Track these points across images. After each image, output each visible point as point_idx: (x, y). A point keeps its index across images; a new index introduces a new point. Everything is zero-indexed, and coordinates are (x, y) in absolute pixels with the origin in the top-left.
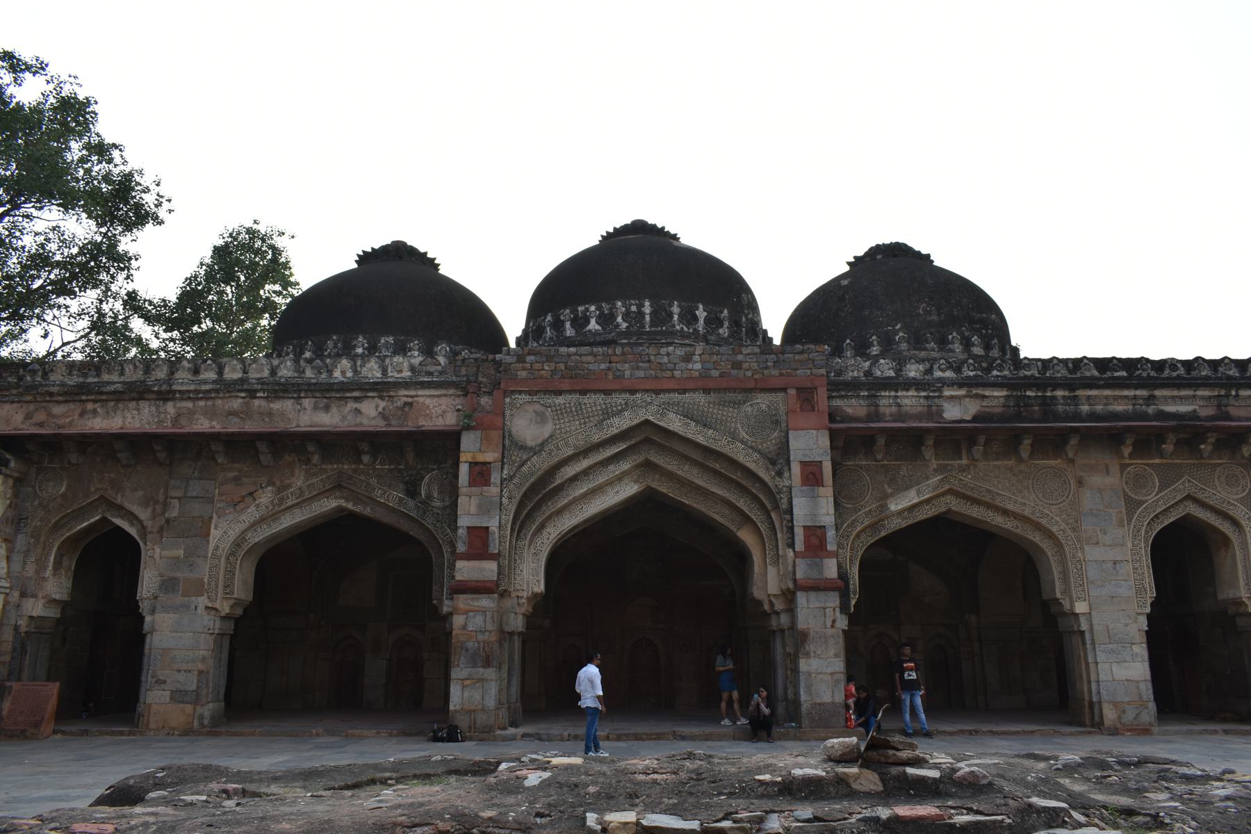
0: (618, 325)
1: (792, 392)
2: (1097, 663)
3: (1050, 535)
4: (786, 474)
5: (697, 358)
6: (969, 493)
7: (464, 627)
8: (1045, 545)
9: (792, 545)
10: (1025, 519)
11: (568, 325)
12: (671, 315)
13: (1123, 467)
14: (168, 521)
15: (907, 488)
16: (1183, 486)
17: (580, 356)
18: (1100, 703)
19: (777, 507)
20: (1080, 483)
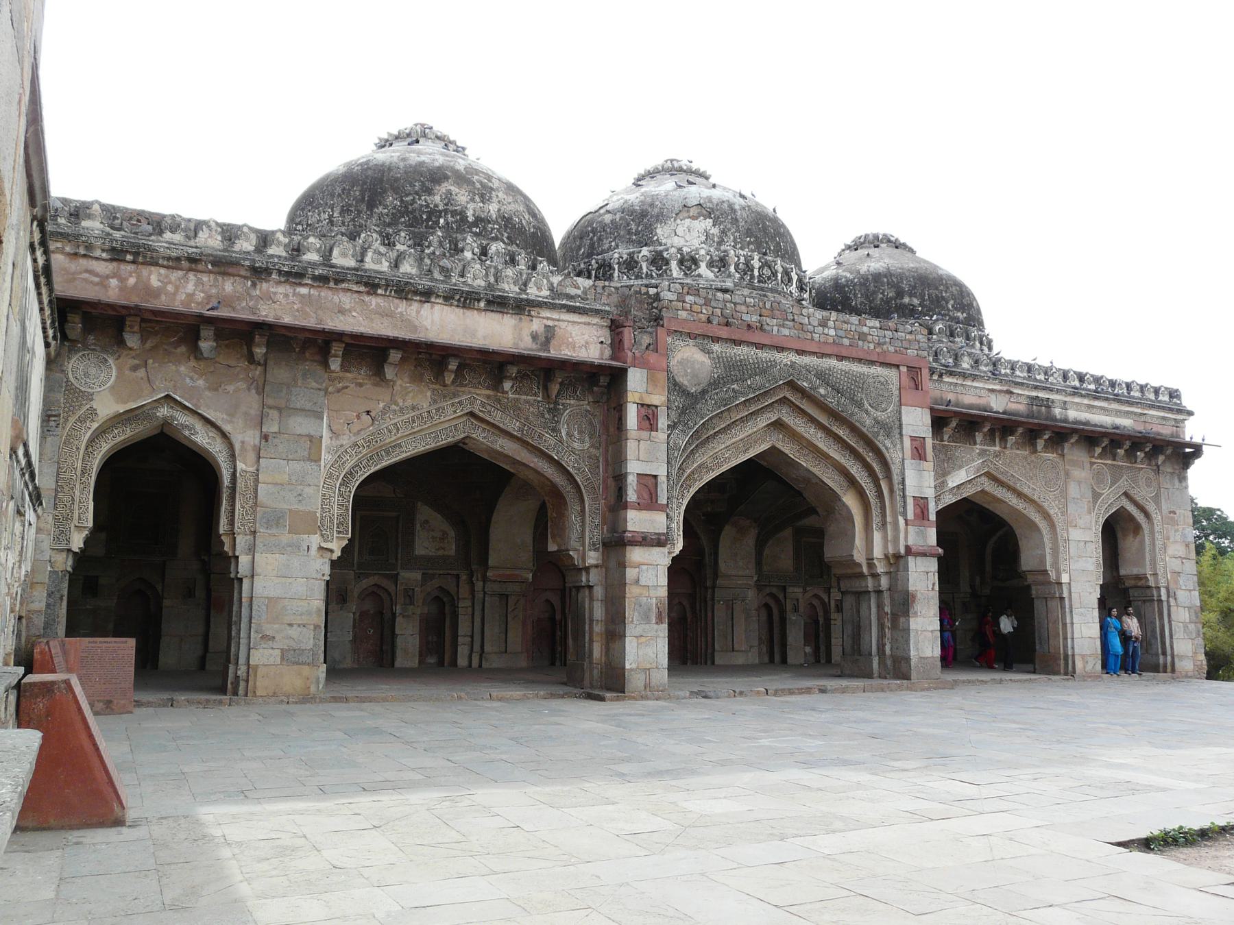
0: (729, 276)
2: (1072, 623)
3: (1047, 516)
4: (899, 447)
5: (831, 324)
6: (1000, 476)
7: (637, 581)
9: (904, 514)
10: (1033, 502)
11: (674, 264)
12: (774, 274)
13: (1092, 464)
14: (265, 437)
15: (961, 467)
16: (1123, 484)
17: (735, 304)
18: (1073, 655)
19: (889, 476)
20: (1067, 474)
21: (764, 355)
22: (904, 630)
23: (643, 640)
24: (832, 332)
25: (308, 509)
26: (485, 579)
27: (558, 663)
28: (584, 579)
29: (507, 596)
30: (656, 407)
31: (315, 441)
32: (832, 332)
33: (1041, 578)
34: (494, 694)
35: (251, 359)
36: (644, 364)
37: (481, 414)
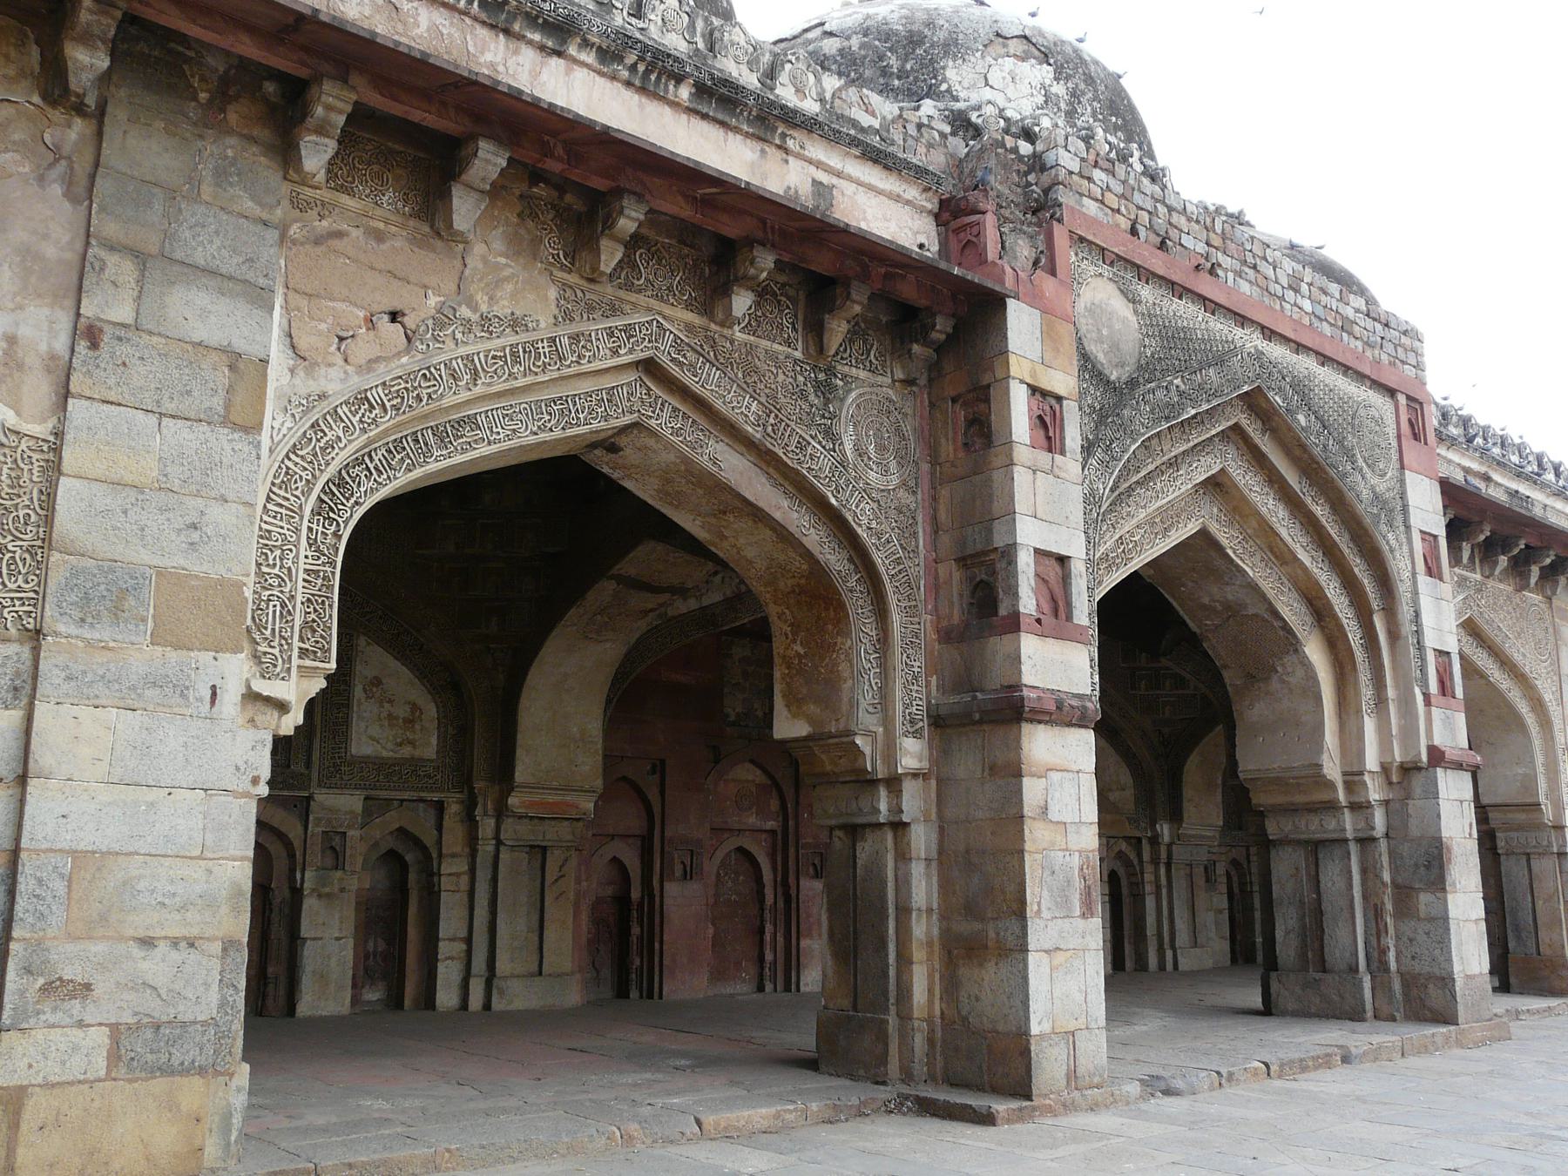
1: (1402, 399)
3: (1538, 705)
8: (1530, 719)
14: (91, 335)
19: (1390, 611)
21: (1220, 327)
22: (1431, 919)
23: (1060, 958)
24: (1307, 305)
25: (216, 571)
26: (501, 811)
27: (634, 994)
28: (883, 806)
29: (544, 849)
30: (1059, 399)
31: (245, 370)
32: (1307, 305)
33: (1521, 817)
34: (709, 1120)
35: (54, 86)
36: (1035, 300)
37: (675, 370)
